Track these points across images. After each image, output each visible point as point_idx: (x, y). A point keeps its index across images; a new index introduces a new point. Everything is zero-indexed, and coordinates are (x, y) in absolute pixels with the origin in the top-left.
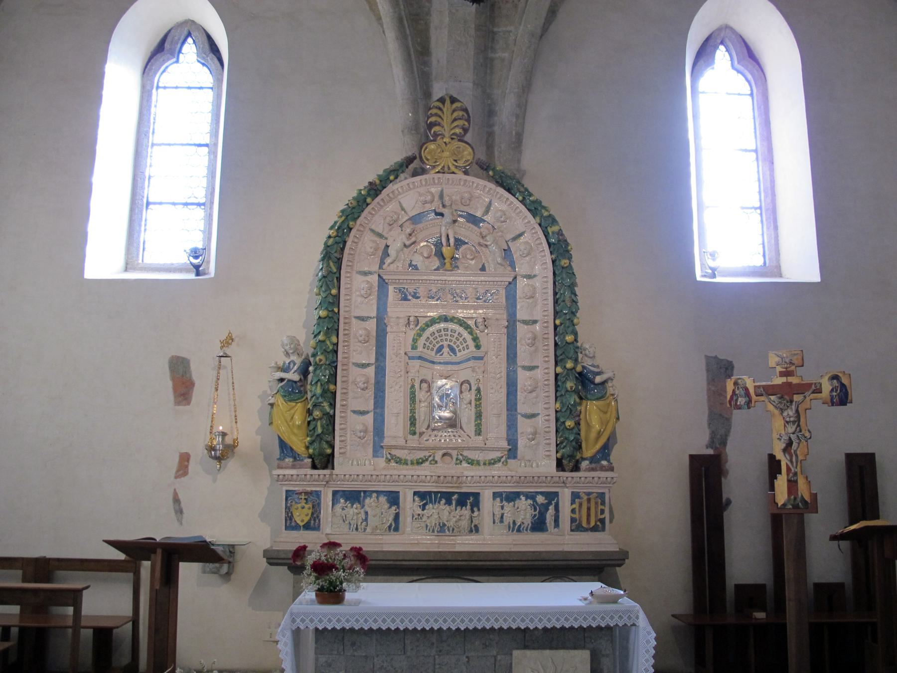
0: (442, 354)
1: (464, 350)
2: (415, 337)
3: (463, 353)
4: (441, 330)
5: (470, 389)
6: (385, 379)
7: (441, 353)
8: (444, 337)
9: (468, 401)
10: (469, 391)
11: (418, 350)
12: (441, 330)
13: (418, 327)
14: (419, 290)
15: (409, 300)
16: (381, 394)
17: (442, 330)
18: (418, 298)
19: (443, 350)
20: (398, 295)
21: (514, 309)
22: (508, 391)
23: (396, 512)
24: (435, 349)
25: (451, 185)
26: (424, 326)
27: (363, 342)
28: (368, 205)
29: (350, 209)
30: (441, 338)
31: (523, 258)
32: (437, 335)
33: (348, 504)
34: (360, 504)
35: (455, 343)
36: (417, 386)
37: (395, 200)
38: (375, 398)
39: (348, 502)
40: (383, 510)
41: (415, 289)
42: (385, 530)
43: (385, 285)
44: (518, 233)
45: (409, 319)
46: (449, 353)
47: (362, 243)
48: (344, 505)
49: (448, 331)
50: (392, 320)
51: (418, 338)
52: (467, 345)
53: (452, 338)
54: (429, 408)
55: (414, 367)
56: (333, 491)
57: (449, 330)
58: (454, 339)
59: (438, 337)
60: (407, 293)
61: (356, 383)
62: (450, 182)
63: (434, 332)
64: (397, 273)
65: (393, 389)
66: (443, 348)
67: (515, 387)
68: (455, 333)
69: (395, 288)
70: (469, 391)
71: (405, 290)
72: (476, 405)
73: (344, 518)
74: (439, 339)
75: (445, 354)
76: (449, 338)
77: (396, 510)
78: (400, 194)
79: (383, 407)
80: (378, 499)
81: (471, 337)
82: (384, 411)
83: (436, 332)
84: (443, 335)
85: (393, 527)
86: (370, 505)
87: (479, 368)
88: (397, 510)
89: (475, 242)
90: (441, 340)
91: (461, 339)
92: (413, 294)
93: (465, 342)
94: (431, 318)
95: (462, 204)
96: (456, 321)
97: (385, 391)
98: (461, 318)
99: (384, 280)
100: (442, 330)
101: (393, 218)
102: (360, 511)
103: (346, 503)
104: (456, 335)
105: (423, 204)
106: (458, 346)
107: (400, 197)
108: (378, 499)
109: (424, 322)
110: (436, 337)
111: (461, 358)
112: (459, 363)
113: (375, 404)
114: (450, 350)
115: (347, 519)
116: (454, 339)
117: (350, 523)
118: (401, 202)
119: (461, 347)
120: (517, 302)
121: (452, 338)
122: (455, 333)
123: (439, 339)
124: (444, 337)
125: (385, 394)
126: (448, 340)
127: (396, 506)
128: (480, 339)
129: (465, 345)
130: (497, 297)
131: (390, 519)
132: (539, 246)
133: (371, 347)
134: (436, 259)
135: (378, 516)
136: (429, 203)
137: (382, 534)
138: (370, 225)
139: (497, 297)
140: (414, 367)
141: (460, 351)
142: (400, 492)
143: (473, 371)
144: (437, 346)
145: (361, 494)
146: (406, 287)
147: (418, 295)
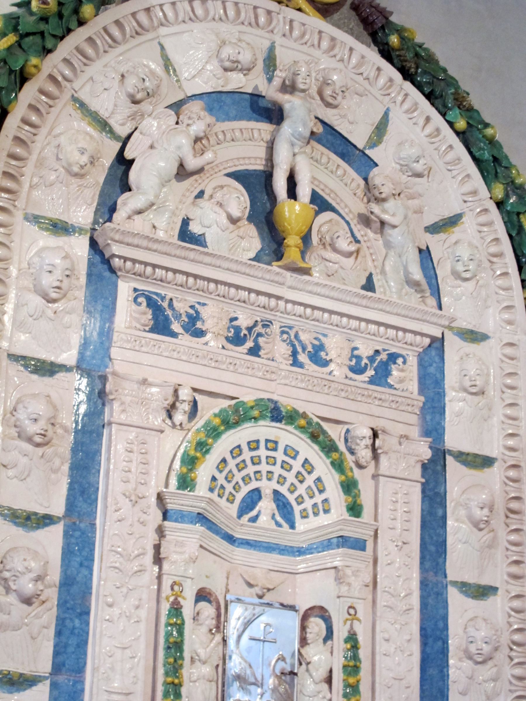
0: (257, 516)
1: (316, 514)
2: (192, 453)
3: (314, 522)
4: (258, 442)
5: (329, 635)
6: (91, 574)
7: (254, 513)
8: (264, 468)
9: (322, 673)
10: (325, 640)
11: (196, 493)
12: (258, 442)
13: (199, 423)
14: (204, 312)
15: (174, 335)
16: (77, 622)
17: (262, 444)
18: (200, 334)
19: (260, 504)
20: (145, 313)
21: (437, 417)
22: (423, 652)
24: (239, 496)
25: (295, 41)
26: (217, 421)
27: (38, 439)
28: (81, 23)
29: (34, 18)
30: (257, 468)
31: (459, 282)
32: (247, 455)
35: (292, 489)
36: (188, 611)
37: (150, 36)
38: (59, 633)
41: (192, 307)
43: (107, 274)
44: (447, 214)
45: (176, 391)
46: (273, 517)
47: (49, 133)
49: (275, 449)
50: (127, 385)
51: (198, 455)
52: (326, 501)
53: (284, 473)
54: (214, 684)
55: (181, 544)
57: (281, 448)
58: (291, 477)
59: (249, 462)
60: (169, 312)
61: (7, 574)
62: (296, 33)
63: (239, 446)
64: (155, 246)
65: (116, 611)
66: (260, 498)
67: (440, 643)
68: (294, 458)
69: (135, 290)
70: (325, 640)
71: (165, 304)
72: (347, 685)
74: (251, 469)
75: (264, 519)
76: (277, 470)
78: (165, 22)
79: (80, 670)
81: (337, 477)
82: (83, 682)
83: (245, 447)
84: (263, 460)
87: (356, 573)
89: (350, 211)
90: (256, 472)
91: (310, 480)
92: (184, 318)
93: (321, 491)
94: (233, 402)
95: (322, 99)
96: (303, 422)
97: (88, 613)
98: (316, 420)
99: (107, 262)
100: (262, 444)
101: (147, 84)
104: (297, 465)
105: (226, 70)
106: (300, 500)
107: (163, 31)
109: (217, 411)
110: (244, 461)
111: (303, 538)
112: (300, 552)
113: (56, 654)
114: (278, 506)
116: (291, 477)
118: (166, 46)
119: (308, 504)
120: (447, 399)
121: (284, 473)
122: (294, 458)
123: (251, 469)
124: (264, 468)
125: (88, 624)
126: (276, 476)
128: (360, 486)
129: (319, 499)
130: (402, 374)
132: (495, 260)
133: (57, 462)
134: (252, 230)
136: (241, 70)
138: (76, 85)
139: (402, 374)
140: (181, 544)
141: (305, 516)
143: (339, 580)
144: (245, 490)
146: (170, 295)
147: (199, 325)
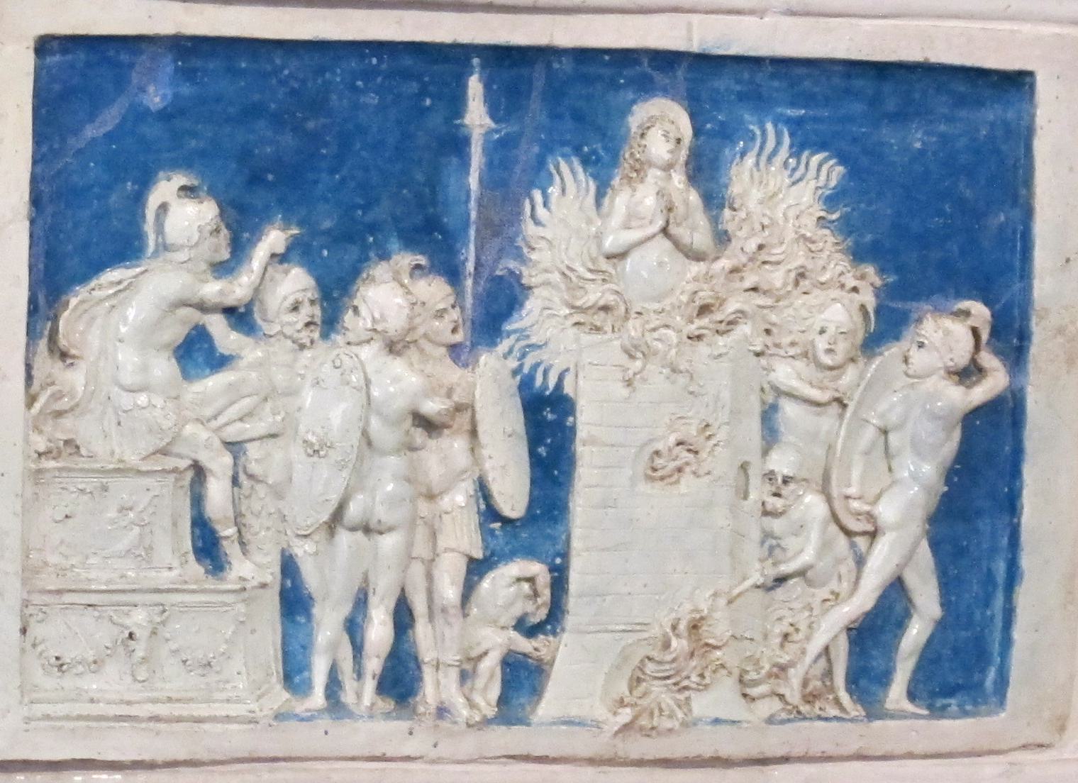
23: (981, 393)
33: (280, 259)
34: (453, 275)
39: (274, 239)
40: (785, 373)
42: (810, 698)
48: (212, 289)
56: (44, 45)
73: (217, 493)
77: (968, 373)
80: (714, 201)
85: (916, 633)
86: (594, 295)
88: (988, 359)
102: (453, 374)
103: (239, 248)
108: (714, 201)
115: (259, 502)
117: (289, 567)
127: (980, 312)
131: (887, 511)
135: (720, 462)
137: (775, 741)
142: (1045, 89)
145: (457, 103)
